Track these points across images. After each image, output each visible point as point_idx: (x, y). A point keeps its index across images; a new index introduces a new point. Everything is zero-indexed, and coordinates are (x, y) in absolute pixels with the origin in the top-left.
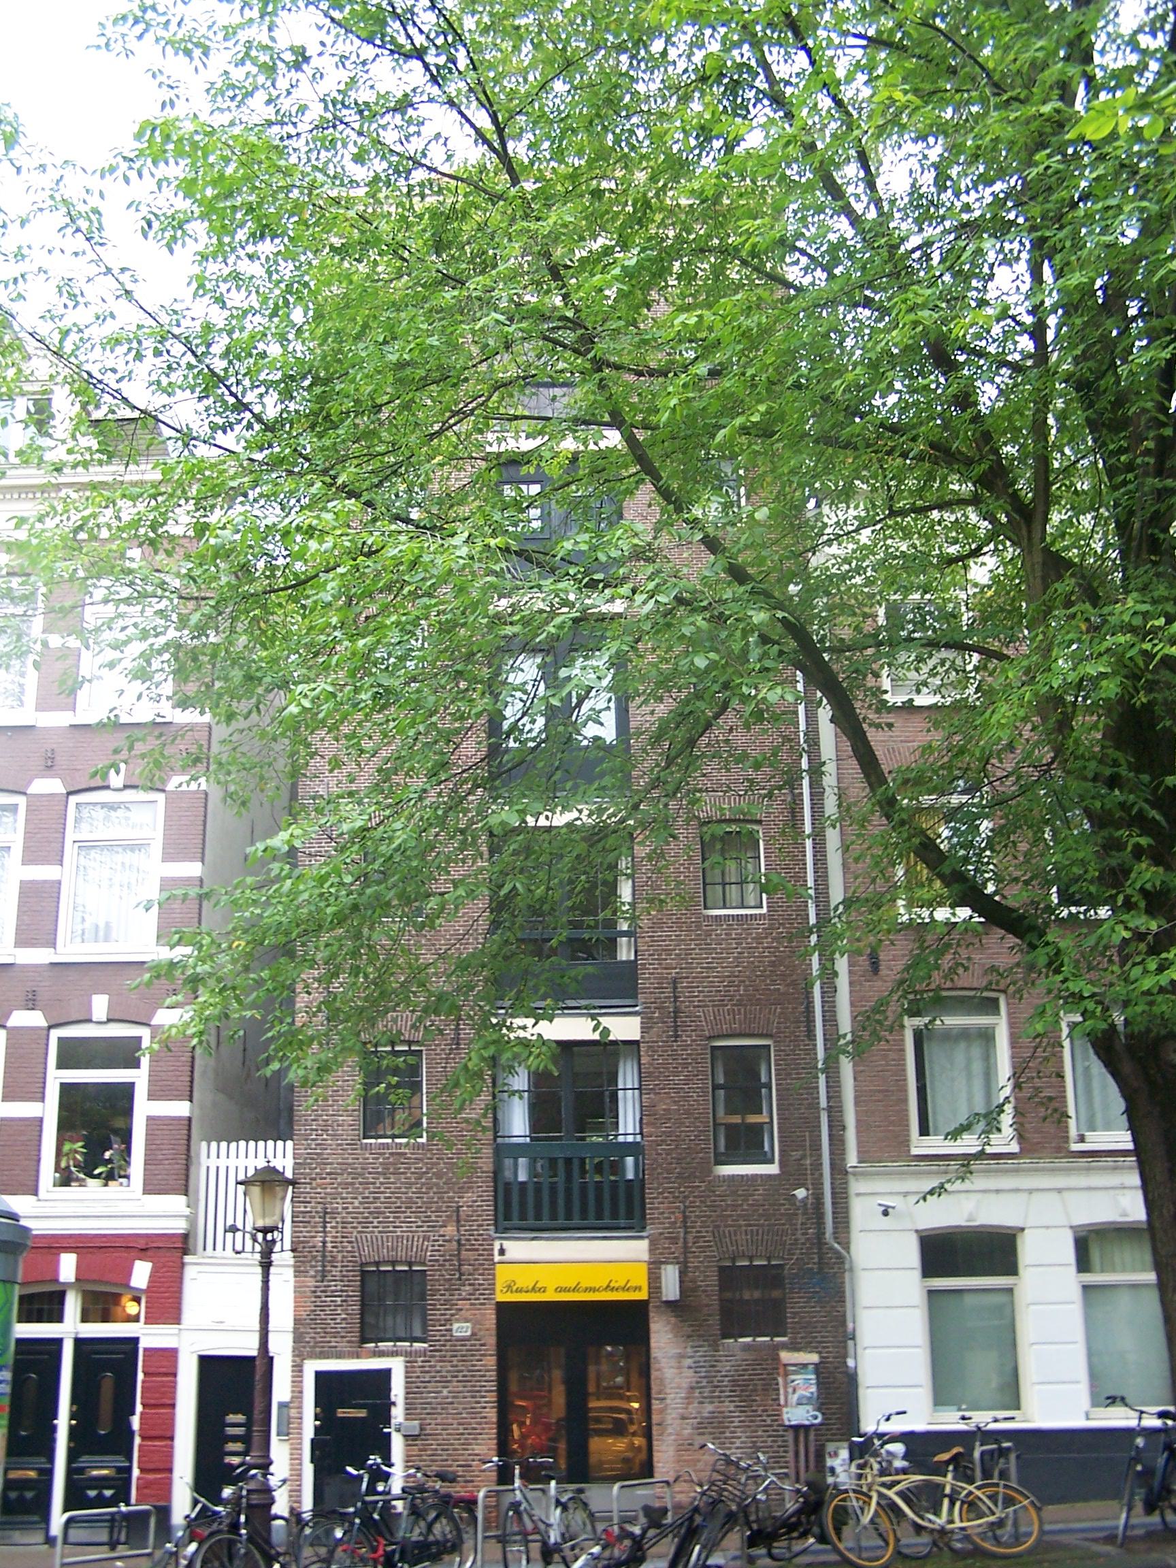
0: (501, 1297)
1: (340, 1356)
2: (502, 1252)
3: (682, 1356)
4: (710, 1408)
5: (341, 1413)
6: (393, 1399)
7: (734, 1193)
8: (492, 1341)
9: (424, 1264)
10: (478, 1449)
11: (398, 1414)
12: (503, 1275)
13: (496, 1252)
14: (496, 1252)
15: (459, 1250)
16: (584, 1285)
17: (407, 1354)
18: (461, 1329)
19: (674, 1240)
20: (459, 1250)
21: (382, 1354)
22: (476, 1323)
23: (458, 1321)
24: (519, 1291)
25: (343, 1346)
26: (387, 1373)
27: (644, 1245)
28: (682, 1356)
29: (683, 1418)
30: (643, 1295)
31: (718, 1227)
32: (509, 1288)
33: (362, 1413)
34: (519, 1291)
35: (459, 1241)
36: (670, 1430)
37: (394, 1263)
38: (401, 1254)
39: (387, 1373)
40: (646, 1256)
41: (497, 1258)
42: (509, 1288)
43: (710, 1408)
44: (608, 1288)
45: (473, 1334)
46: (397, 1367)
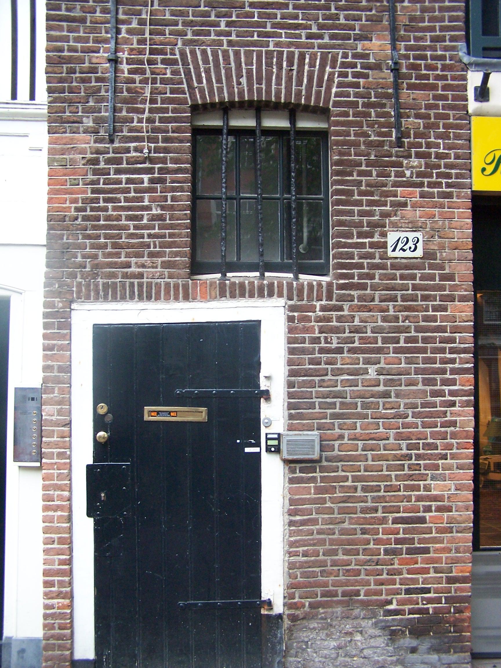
0: (481, 183)
1: (148, 294)
2: (483, 93)
5: (151, 413)
6: (263, 385)
8: (464, 269)
9: (322, 112)
10: (437, 488)
11: (274, 415)
13: (471, 94)
14: (471, 94)
15: (397, 86)
17: (292, 292)
18: (403, 243)
20: (397, 86)
21: (240, 291)
22: (435, 232)
23: (396, 226)
25: (155, 273)
26: (250, 331)
33: (199, 415)
35: (396, 70)
37: (259, 108)
38: (278, 90)
39: (250, 331)
41: (473, 105)
45: (428, 255)
46: (271, 317)
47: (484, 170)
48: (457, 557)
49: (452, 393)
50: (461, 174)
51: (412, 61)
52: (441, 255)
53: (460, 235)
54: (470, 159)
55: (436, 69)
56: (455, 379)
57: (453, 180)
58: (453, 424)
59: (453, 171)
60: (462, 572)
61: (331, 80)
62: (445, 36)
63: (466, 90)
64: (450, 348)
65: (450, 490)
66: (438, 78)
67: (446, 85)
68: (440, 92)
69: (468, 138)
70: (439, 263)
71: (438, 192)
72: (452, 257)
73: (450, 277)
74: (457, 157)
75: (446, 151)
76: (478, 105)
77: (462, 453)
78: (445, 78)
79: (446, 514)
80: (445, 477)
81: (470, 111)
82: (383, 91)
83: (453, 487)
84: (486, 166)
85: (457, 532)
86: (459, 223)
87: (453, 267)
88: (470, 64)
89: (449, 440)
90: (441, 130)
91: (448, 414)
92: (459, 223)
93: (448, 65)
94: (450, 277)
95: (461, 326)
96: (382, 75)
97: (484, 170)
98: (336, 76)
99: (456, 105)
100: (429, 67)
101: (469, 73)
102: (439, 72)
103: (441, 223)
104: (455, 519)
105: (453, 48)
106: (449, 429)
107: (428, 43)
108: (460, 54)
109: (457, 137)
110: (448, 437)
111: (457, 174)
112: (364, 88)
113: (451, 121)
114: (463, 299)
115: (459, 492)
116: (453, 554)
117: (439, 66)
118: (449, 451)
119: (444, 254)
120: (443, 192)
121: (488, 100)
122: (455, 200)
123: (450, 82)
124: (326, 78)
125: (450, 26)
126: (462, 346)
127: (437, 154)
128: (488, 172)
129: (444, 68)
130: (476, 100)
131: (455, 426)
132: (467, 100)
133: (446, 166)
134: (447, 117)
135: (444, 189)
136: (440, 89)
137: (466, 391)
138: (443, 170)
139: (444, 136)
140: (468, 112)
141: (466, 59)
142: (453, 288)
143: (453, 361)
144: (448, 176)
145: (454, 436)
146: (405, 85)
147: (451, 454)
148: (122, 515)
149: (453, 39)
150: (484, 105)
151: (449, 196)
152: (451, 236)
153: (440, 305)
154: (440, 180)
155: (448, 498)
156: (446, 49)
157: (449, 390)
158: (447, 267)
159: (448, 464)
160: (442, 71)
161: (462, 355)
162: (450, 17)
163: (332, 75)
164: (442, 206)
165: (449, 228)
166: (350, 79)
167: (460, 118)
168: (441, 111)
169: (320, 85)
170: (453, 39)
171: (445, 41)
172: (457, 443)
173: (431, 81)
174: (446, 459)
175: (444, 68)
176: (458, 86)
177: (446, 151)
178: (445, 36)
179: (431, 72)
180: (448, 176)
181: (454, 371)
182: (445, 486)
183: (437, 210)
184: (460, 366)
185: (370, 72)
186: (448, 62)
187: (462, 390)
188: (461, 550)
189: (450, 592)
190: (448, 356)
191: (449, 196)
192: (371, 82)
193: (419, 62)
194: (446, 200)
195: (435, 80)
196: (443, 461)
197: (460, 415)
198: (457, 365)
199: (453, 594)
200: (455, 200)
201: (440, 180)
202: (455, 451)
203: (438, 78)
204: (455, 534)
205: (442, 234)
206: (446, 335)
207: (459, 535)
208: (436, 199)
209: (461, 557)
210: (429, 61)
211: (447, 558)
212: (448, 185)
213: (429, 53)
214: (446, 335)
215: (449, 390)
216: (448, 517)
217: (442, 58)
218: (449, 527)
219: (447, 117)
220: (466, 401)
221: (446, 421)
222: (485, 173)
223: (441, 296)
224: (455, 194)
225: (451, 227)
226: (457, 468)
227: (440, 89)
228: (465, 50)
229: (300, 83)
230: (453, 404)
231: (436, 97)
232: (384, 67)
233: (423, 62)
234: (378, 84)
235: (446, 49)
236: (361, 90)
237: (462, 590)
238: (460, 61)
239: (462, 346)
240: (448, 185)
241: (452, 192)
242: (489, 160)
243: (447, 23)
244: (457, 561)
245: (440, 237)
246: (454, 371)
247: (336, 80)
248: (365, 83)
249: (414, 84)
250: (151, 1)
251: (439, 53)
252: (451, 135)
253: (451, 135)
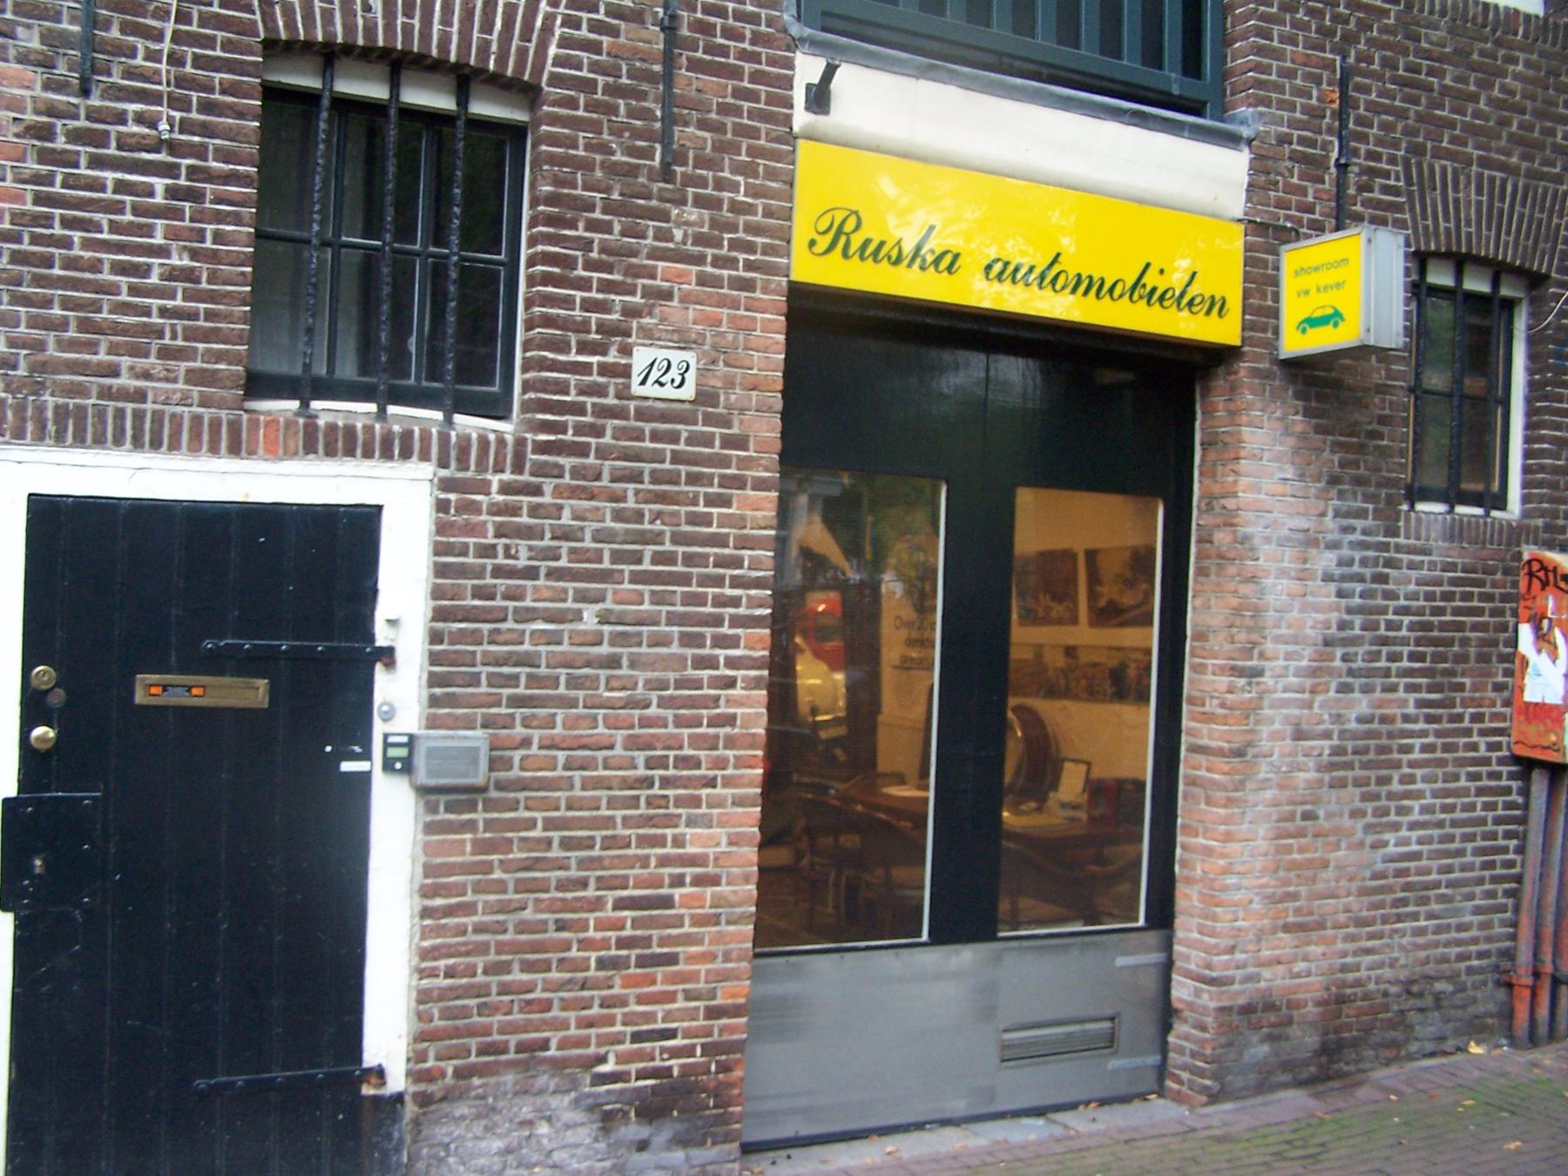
1: (154, 435)
2: (819, 98)
3: (1310, 541)
4: (1362, 704)
5: (147, 689)
6: (382, 636)
8: (766, 429)
9: (529, 93)
10: (696, 841)
11: (400, 697)
12: (819, 187)
13: (799, 96)
14: (799, 96)
15: (669, 59)
16: (1070, 266)
17: (451, 453)
18: (661, 370)
19: (1313, 165)
20: (669, 59)
21: (342, 443)
22: (718, 353)
23: (648, 335)
24: (874, 252)
25: (171, 391)
26: (360, 526)
27: (1234, 165)
28: (1310, 541)
29: (1299, 735)
30: (1224, 330)
31: (1418, 150)
32: (838, 237)
33: (255, 693)
34: (874, 252)
35: (669, 28)
36: (1264, 772)
37: (398, 64)
38: (444, 35)
39: (360, 526)
40: (1237, 205)
41: (801, 118)
42: (838, 237)
43: (1362, 704)
44: (1139, 290)
45: (705, 397)
46: (404, 502)
47: (812, 243)
48: (725, 970)
49: (732, 663)
50: (772, 246)
51: (699, 15)
52: (727, 399)
53: (763, 365)
55: (741, 38)
57: (758, 257)
58: (730, 720)
60: (733, 996)
61: (547, 29)
63: (791, 88)
64: (733, 578)
67: (757, 71)
68: (746, 84)
72: (746, 404)
73: (740, 442)
74: (768, 213)
81: (796, 128)
82: (645, 66)
83: (724, 840)
84: (816, 237)
85: (729, 923)
88: (802, 40)
91: (722, 702)
94: (740, 442)
96: (645, 34)
97: (812, 243)
98: (559, 22)
99: (772, 113)
100: (729, 33)
101: (798, 54)
102: (746, 45)
103: (730, 337)
108: (786, 17)
109: (771, 174)
110: (721, 745)
112: (609, 54)
114: (760, 485)
115: (734, 849)
116: (719, 965)
117: (748, 35)
119: (733, 397)
122: (758, 295)
124: (539, 23)
127: (733, 202)
129: (757, 39)
130: (808, 108)
132: (791, 107)
133: (749, 228)
135: (741, 273)
136: (746, 77)
137: (755, 659)
138: (741, 235)
139: (748, 170)
141: (796, 30)
142: (745, 463)
143: (735, 602)
144: (750, 248)
145: (731, 743)
146: (684, 60)
147: (723, 777)
148: (79, 904)
150: (821, 118)
151: (748, 285)
152: (747, 363)
155: (716, 859)
158: (736, 423)
159: (719, 795)
161: (753, 592)
163: (550, 18)
164: (735, 305)
165: (746, 348)
166: (584, 33)
167: (778, 140)
169: (526, 36)
174: (714, 786)
175: (757, 39)
176: (779, 77)
180: (750, 248)
181: (736, 621)
182: (711, 837)
183: (726, 311)
184: (748, 612)
185: (623, 25)
186: (763, 28)
187: (750, 658)
188: (734, 955)
191: (748, 285)
192: (624, 46)
193: (712, 19)
195: (739, 59)
196: (709, 791)
197: (742, 705)
198: (742, 611)
199: (716, 1037)
200: (758, 295)
201: (734, 254)
206: (726, 551)
207: (732, 928)
208: (725, 291)
209: (733, 969)
210: (731, 21)
212: (749, 266)
214: (726, 551)
216: (713, 895)
223: (722, 476)
224: (759, 284)
226: (733, 803)
227: (746, 77)
228: (794, 12)
229: (487, 27)
230: (730, 683)
232: (649, 20)
233: (719, 21)
234: (636, 51)
236: (604, 57)
238: (785, 31)
240: (749, 266)
241: (753, 280)
242: (823, 226)
244: (724, 976)
245: (727, 364)
246: (736, 621)
247: (558, 32)
248: (612, 45)
249: (700, 61)
250: (485, 4)
252: (761, 169)
253: (761, 169)
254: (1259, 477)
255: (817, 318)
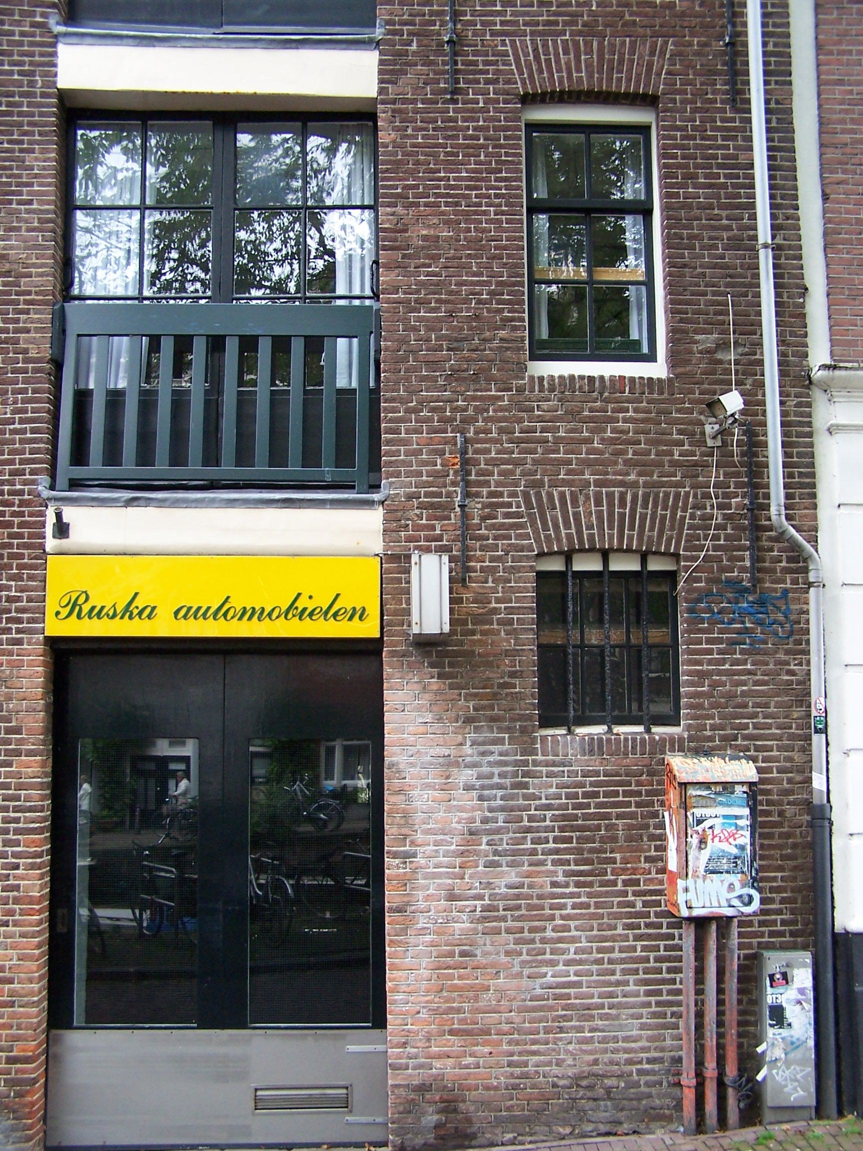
0: (56, 628)
2: (62, 530)
3: (450, 763)
4: (512, 876)
7: (573, 415)
12: (62, 577)
13: (49, 530)
14: (49, 530)
16: (237, 603)
19: (439, 510)
24: (97, 613)
27: (375, 518)
28: (450, 763)
29: (452, 897)
30: (368, 628)
31: (539, 484)
32: (74, 608)
34: (97, 613)
36: (422, 922)
40: (378, 545)
41: (51, 543)
42: (74, 608)
43: (512, 876)
44: (292, 610)
47: (58, 613)
48: (18, 1034)
49: (15, 855)
50: (33, 618)
52: (8, 707)
53: (29, 685)
54: (44, 601)
55: (13, 505)
56: (19, 840)
57: (25, 625)
58: (17, 888)
59: (25, 615)
60: (23, 1051)
62: (24, 469)
64: (14, 807)
65: (11, 960)
66: (14, 514)
67: (22, 521)
68: (16, 530)
69: (42, 579)
70: (5, 716)
71: (7, 639)
72: (19, 708)
73: (17, 730)
74: (30, 600)
75: (18, 594)
76: (57, 542)
77: (25, 920)
78: (22, 514)
79: (7, 986)
80: (6, 946)
81: (48, 549)
83: (15, 957)
84: (60, 609)
85: (20, 1006)
86: (28, 672)
87: (20, 720)
88: (49, 499)
89: (11, 906)
90: (15, 571)
91: (11, 877)
92: (28, 672)
93: (26, 500)
94: (17, 730)
95: (26, 782)
97: (58, 613)
99: (31, 543)
103: (8, 672)
104: (17, 992)
105: (33, 482)
106: (11, 894)
107: (7, 477)
108: (40, 488)
109: (31, 578)
110: (11, 902)
111: (28, 618)
113: (26, 561)
114: (30, 753)
115: (21, 962)
116: (13, 1032)
117: (17, 502)
118: (11, 918)
119: (11, 706)
120: (13, 638)
121: (68, 537)
122: (25, 646)
123: (27, 519)
125: (31, 459)
126: (28, 804)
127: (8, 597)
128: (61, 616)
129: (22, 503)
130: (54, 537)
131: (18, 891)
132: (44, 538)
133: (18, 610)
134: (22, 557)
135: (14, 636)
137: (31, 853)
138: (14, 614)
139: (17, 578)
140: (44, 550)
141: (46, 493)
142: (20, 742)
143: (17, 820)
144: (19, 621)
145: (16, 901)
147: (13, 921)
149: (33, 472)
150: (64, 541)
151: (19, 642)
152: (19, 685)
153: (5, 760)
154: (10, 625)
155: (10, 968)
156: (25, 483)
157: (12, 852)
158: (14, 719)
159: (11, 931)
160: (18, 507)
161: (27, 814)
162: (30, 449)
164: (11, 653)
165: (18, 677)
167: (35, 558)
168: (15, 550)
170: (33, 472)
171: (25, 475)
172: (20, 909)
173: (7, 519)
174: (8, 926)
175: (22, 503)
177: (18, 594)
178: (24, 469)
179: (7, 509)
180: (19, 621)
181: (17, 831)
182: (6, 955)
183: (5, 658)
184: (25, 826)
186: (26, 497)
187: (27, 851)
188: (23, 1026)
189: (10, 1074)
190: (12, 815)
191: (19, 642)
194: (15, 647)
196: (5, 928)
197: (23, 879)
198: (21, 825)
199: (13, 1075)
200: (25, 646)
201: (10, 625)
202: (17, 917)
203: (14, 514)
204: (16, 1009)
205: (9, 684)
206: (10, 792)
207: (21, 1009)
208: (5, 647)
209: (23, 1034)
210: (6, 497)
211: (7, 1035)
212: (19, 631)
213: (6, 488)
214: (10, 792)
215: (12, 852)
216: (9, 989)
217: (21, 493)
218: (10, 1001)
219: (22, 557)
220: (31, 863)
221: (8, 885)
222: (59, 617)
223: (6, 750)
224: (25, 640)
225: (20, 675)
226: (20, 936)
230: (16, 867)
231: (11, 536)
235: (25, 483)
237: (24, 1071)
239: (28, 804)
240: (19, 631)
241: (22, 639)
242: (64, 603)
243: (27, 456)
244: (18, 1038)
245: (6, 687)
246: (17, 831)
251: (18, 487)
252: (25, 576)
253: (25, 576)
254: (412, 720)
255: (64, 654)
